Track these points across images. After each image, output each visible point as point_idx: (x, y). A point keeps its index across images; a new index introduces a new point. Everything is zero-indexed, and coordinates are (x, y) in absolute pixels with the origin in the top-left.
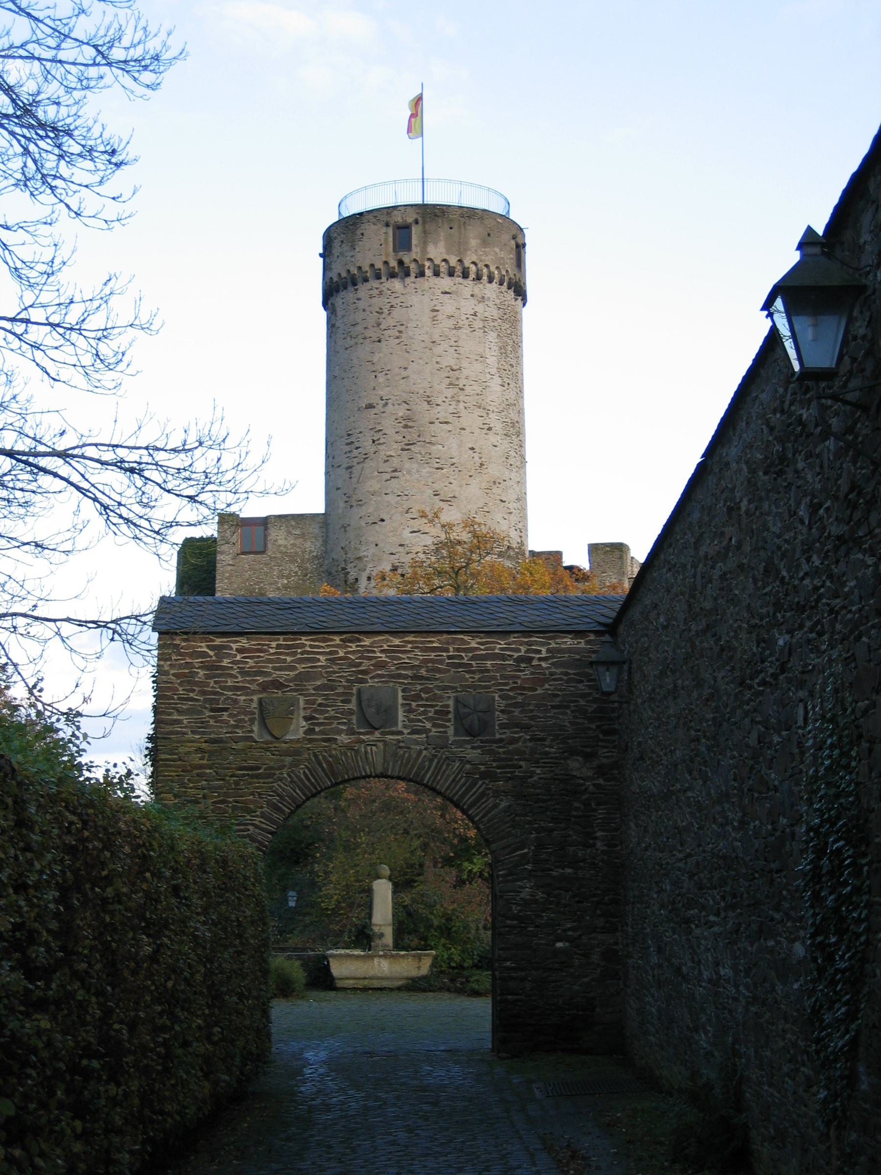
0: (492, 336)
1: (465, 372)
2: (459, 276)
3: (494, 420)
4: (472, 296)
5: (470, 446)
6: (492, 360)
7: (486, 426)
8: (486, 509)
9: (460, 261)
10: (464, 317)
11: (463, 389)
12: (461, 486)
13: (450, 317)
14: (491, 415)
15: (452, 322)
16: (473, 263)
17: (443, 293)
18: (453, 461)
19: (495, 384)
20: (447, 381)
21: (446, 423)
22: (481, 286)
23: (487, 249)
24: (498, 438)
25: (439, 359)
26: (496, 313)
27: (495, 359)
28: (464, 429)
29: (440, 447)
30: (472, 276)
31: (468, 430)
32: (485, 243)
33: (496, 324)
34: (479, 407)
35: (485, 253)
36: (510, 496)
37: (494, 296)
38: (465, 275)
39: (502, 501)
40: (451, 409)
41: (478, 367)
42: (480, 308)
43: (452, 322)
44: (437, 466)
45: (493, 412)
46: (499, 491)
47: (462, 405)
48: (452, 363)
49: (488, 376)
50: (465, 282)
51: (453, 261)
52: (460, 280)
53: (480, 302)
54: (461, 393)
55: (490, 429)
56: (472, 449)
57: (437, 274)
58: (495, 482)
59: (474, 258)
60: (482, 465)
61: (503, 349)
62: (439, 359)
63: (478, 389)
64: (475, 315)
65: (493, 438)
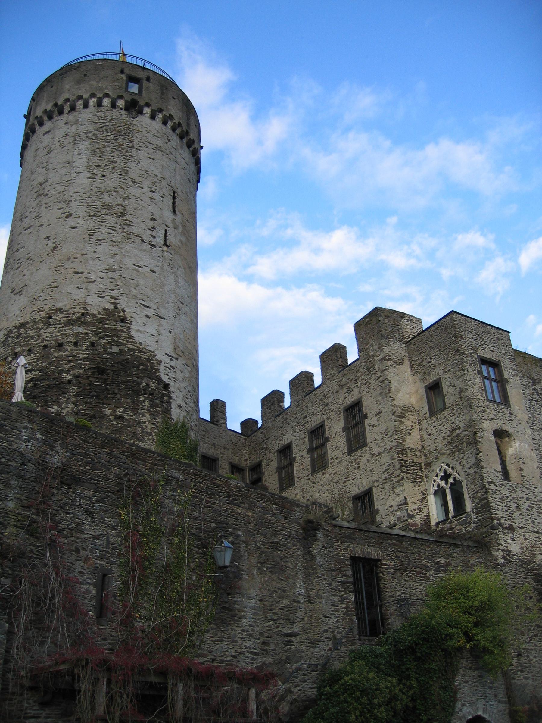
0: (84, 145)
1: (50, 181)
2: (57, 116)
3: (76, 208)
4: (66, 123)
5: (45, 236)
6: (80, 162)
7: (65, 215)
8: (54, 285)
9: (56, 105)
10: (56, 142)
11: (47, 195)
12: (31, 274)
13: (45, 148)
14: (72, 204)
15: (48, 149)
16: (67, 100)
17: (44, 134)
18: (29, 255)
19: (82, 181)
20: (35, 195)
21: (29, 228)
22: (76, 114)
23: (82, 85)
24: (79, 220)
25: (32, 183)
26: (91, 127)
27: (86, 160)
28: (42, 225)
29: (22, 250)
30: (67, 108)
31: (46, 224)
32: (79, 82)
33: (90, 135)
34: (59, 202)
35: (79, 89)
36: (95, 268)
37: (91, 115)
38: (61, 113)
39: (77, 273)
40: (35, 214)
41: (64, 171)
42: (72, 130)
43: (48, 149)
44: (17, 266)
45: (75, 201)
46: (72, 265)
47: (43, 208)
48: (41, 179)
49: (74, 175)
50: (61, 117)
51: (49, 107)
52: (58, 118)
53: (72, 125)
54: (44, 198)
55: (70, 215)
56: (48, 237)
57: (41, 124)
58: (68, 259)
59: (67, 96)
60: (54, 248)
61: (98, 151)
62: (32, 183)
63: (60, 188)
64: (67, 135)
65: (71, 222)
